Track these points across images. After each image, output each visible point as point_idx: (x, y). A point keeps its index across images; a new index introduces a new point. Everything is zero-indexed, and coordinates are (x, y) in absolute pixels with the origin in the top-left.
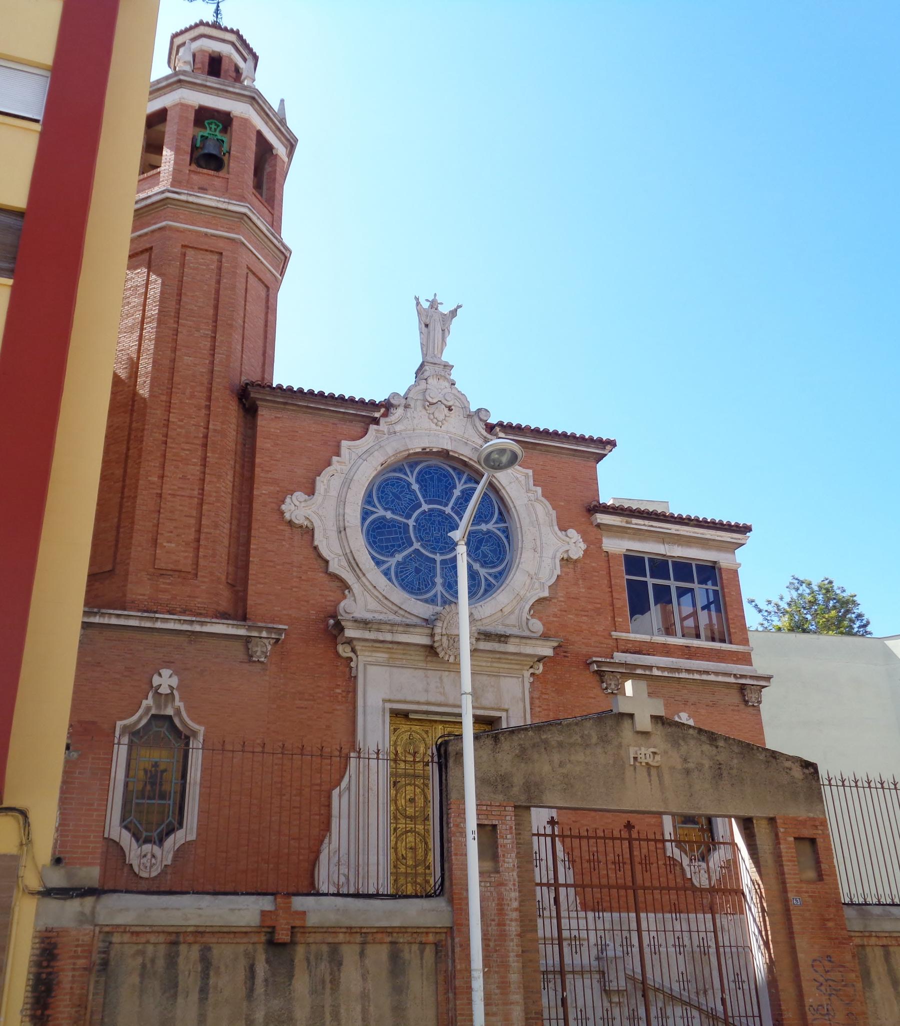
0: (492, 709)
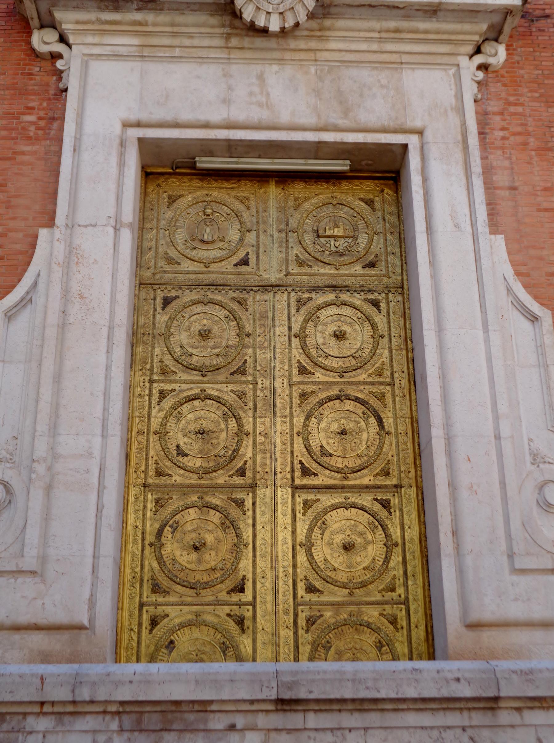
0: (384, 130)
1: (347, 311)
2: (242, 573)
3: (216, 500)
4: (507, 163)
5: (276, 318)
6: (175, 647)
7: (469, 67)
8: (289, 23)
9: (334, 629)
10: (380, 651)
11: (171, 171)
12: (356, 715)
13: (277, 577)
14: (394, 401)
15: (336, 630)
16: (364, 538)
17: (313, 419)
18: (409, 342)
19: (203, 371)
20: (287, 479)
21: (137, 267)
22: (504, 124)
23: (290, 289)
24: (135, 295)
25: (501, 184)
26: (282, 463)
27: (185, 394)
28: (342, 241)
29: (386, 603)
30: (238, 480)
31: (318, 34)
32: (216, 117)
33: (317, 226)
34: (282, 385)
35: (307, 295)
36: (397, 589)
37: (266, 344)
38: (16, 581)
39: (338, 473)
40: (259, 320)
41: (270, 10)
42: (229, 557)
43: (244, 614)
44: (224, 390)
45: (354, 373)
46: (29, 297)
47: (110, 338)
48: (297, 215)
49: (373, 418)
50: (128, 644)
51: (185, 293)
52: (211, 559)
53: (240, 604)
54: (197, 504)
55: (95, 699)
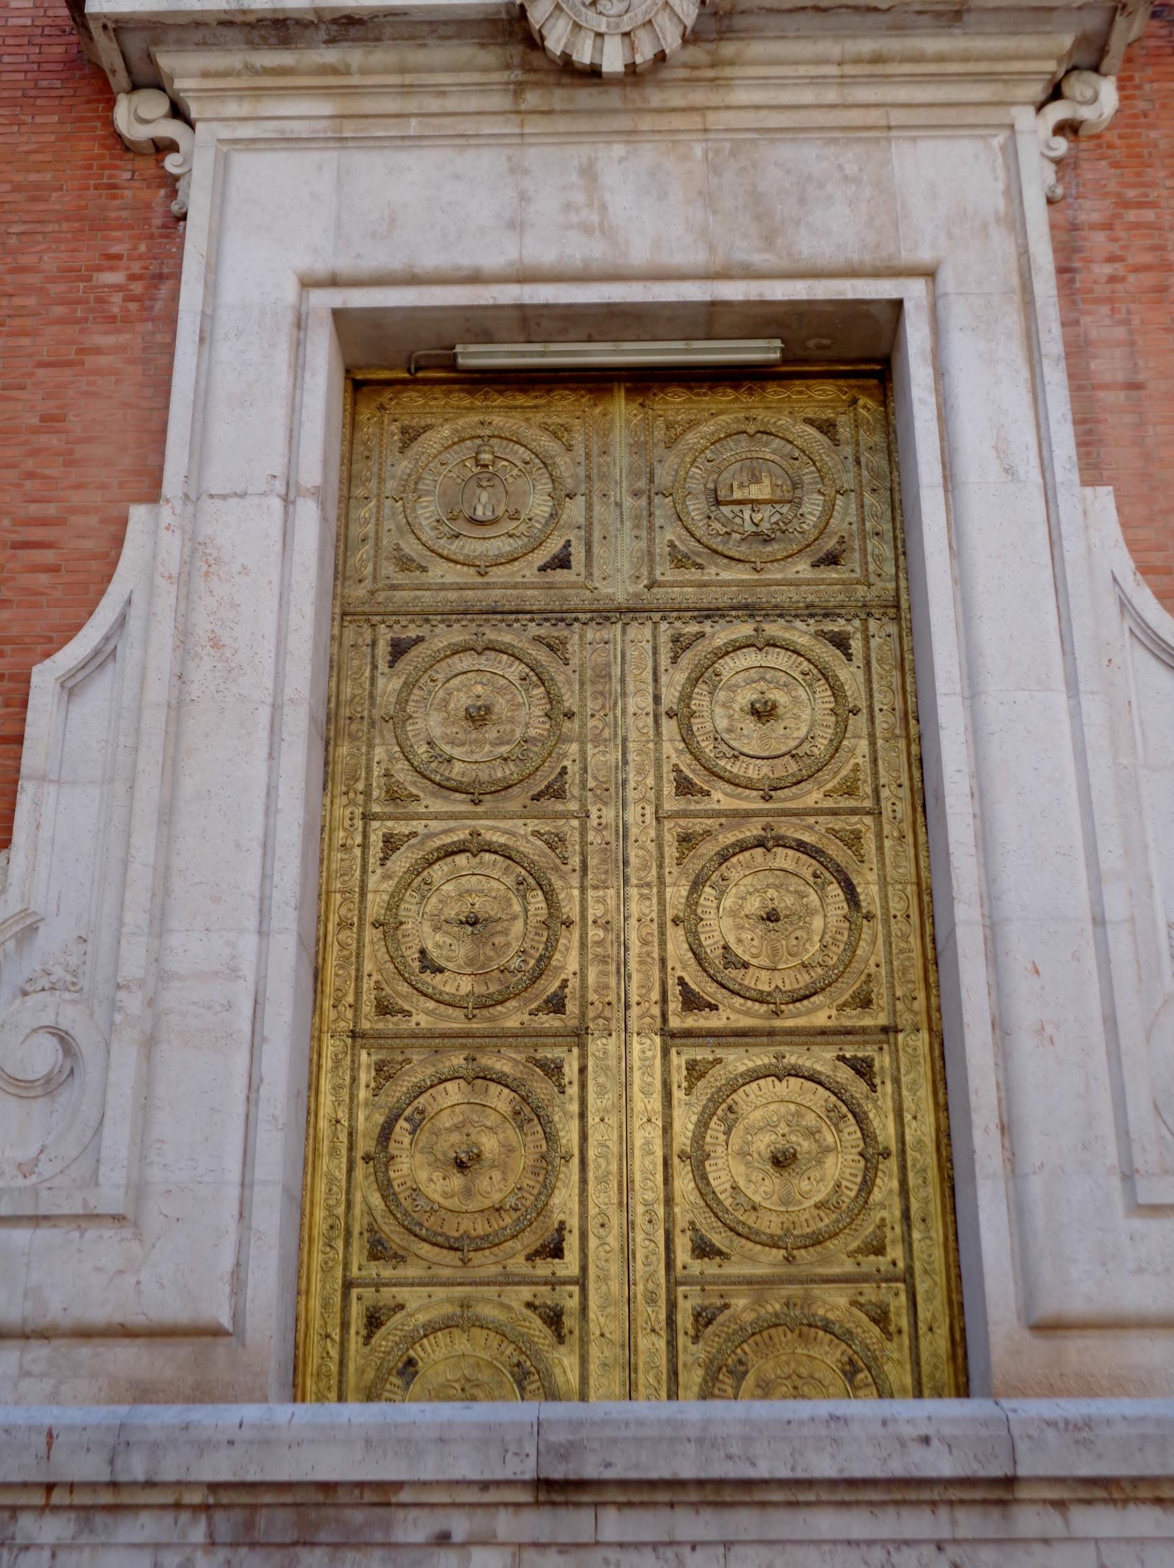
0: (853, 273)
1: (779, 659)
2: (558, 1217)
3: (502, 1065)
4: (1120, 333)
5: (629, 679)
6: (417, 1372)
7: (1036, 131)
8: (645, 54)
9: (753, 1334)
10: (851, 1381)
11: (407, 375)
12: (707, 1514)
13: (631, 1225)
14: (880, 848)
15: (758, 1338)
16: (816, 1141)
17: (707, 889)
18: (912, 722)
19: (474, 792)
20: (652, 1017)
21: (336, 578)
22: (1115, 248)
23: (656, 616)
24: (333, 638)
25: (1107, 378)
26: (641, 985)
27: (438, 843)
28: (767, 511)
29: (865, 1278)
30: (549, 1021)
31: (710, 73)
32: (492, 260)
33: (716, 482)
34: (640, 819)
35: (693, 628)
36: (888, 1249)
37: (606, 734)
38: (82, 1237)
39: (761, 1002)
40: (593, 683)
41: (603, 29)
42: (531, 1183)
43: (562, 1303)
44: (518, 831)
45: (794, 789)
46: (110, 647)
47: (274, 728)
48: (672, 459)
49: (836, 885)
50: (320, 1366)
51: (437, 630)
52: (492, 1187)
53: (554, 1283)
54: (462, 1072)
55: (156, 1479)
